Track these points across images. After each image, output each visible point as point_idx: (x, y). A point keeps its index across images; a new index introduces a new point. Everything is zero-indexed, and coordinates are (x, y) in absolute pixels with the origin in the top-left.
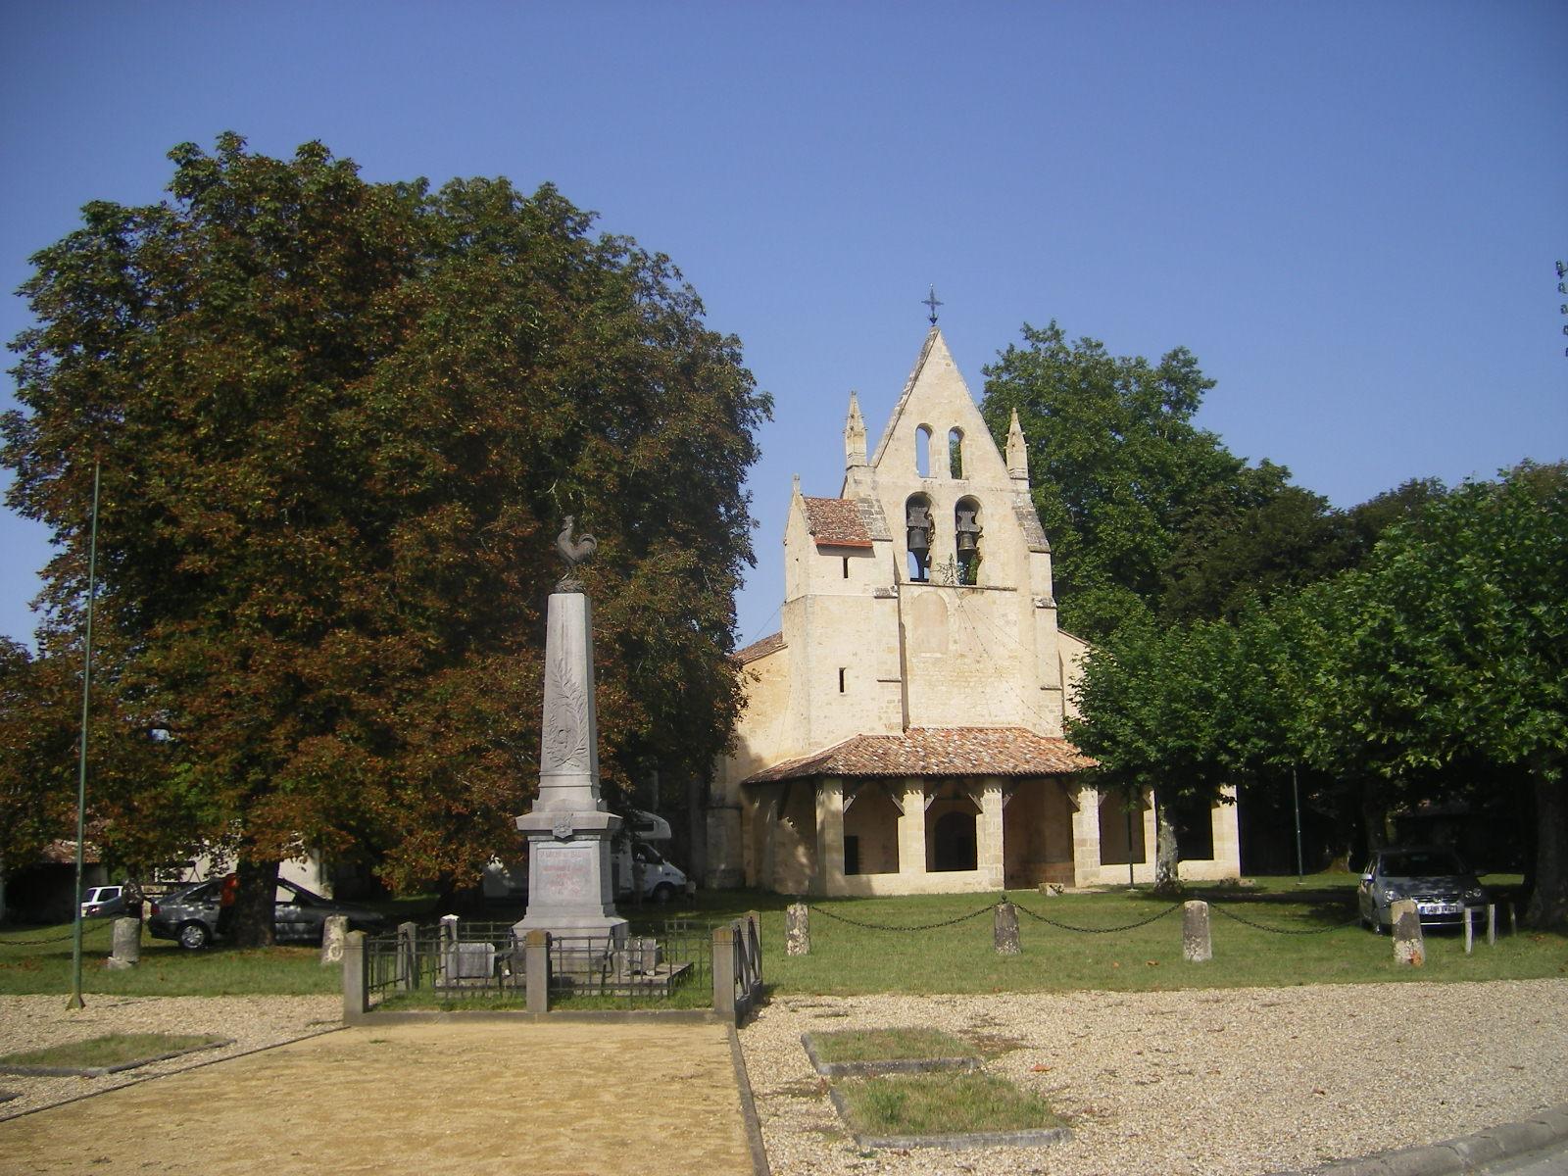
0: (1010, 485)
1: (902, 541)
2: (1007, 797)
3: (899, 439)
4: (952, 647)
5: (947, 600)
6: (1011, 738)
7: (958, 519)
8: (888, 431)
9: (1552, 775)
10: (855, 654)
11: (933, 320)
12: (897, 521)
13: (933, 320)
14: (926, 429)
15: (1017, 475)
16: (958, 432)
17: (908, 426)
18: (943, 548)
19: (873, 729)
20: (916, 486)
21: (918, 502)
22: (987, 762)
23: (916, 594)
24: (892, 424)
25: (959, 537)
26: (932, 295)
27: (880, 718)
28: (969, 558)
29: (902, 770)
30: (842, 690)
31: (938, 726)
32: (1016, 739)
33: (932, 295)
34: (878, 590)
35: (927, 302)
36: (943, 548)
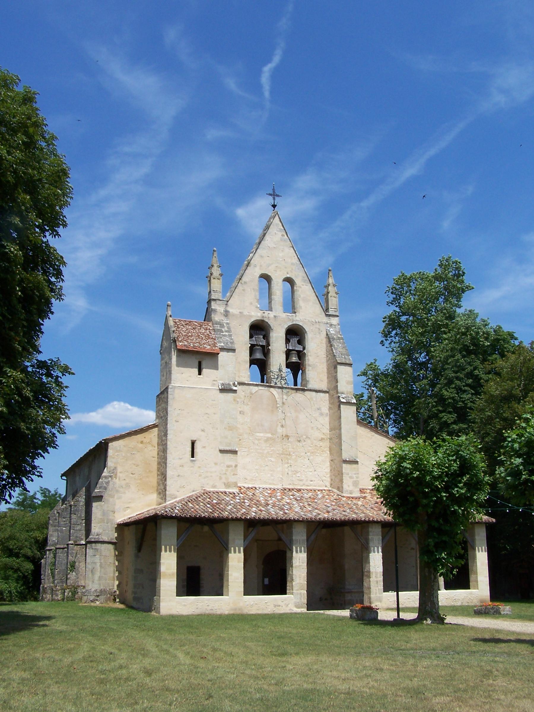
0: (325, 319)
1: (244, 355)
2: (313, 537)
3: (245, 283)
4: (280, 430)
5: (277, 396)
6: (320, 496)
7: (287, 341)
8: (238, 277)
9: (514, 493)
10: (203, 431)
11: (274, 206)
12: (242, 339)
13: (274, 206)
14: (266, 278)
15: (330, 313)
16: (289, 281)
17: (252, 275)
18: (278, 360)
19: (214, 487)
20: (256, 315)
21: (259, 329)
22: (296, 511)
23: (254, 391)
24: (241, 272)
25: (288, 353)
26: (274, 190)
27: (221, 478)
28: (296, 367)
29: (226, 514)
30: (193, 456)
31: (268, 486)
32: (323, 497)
33: (274, 190)
34: (222, 384)
35: (278, 196)
36: (278, 360)
